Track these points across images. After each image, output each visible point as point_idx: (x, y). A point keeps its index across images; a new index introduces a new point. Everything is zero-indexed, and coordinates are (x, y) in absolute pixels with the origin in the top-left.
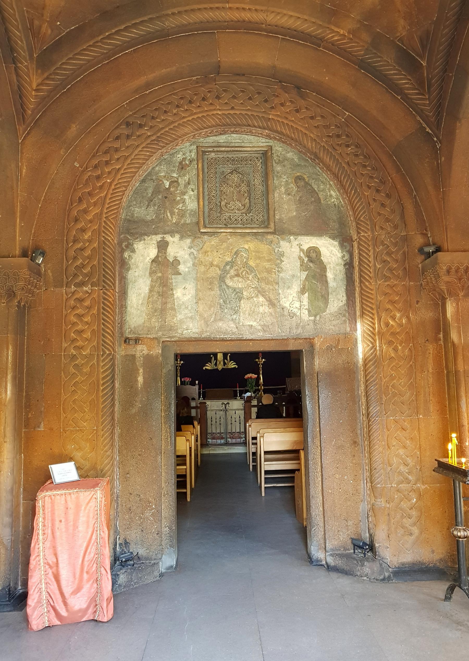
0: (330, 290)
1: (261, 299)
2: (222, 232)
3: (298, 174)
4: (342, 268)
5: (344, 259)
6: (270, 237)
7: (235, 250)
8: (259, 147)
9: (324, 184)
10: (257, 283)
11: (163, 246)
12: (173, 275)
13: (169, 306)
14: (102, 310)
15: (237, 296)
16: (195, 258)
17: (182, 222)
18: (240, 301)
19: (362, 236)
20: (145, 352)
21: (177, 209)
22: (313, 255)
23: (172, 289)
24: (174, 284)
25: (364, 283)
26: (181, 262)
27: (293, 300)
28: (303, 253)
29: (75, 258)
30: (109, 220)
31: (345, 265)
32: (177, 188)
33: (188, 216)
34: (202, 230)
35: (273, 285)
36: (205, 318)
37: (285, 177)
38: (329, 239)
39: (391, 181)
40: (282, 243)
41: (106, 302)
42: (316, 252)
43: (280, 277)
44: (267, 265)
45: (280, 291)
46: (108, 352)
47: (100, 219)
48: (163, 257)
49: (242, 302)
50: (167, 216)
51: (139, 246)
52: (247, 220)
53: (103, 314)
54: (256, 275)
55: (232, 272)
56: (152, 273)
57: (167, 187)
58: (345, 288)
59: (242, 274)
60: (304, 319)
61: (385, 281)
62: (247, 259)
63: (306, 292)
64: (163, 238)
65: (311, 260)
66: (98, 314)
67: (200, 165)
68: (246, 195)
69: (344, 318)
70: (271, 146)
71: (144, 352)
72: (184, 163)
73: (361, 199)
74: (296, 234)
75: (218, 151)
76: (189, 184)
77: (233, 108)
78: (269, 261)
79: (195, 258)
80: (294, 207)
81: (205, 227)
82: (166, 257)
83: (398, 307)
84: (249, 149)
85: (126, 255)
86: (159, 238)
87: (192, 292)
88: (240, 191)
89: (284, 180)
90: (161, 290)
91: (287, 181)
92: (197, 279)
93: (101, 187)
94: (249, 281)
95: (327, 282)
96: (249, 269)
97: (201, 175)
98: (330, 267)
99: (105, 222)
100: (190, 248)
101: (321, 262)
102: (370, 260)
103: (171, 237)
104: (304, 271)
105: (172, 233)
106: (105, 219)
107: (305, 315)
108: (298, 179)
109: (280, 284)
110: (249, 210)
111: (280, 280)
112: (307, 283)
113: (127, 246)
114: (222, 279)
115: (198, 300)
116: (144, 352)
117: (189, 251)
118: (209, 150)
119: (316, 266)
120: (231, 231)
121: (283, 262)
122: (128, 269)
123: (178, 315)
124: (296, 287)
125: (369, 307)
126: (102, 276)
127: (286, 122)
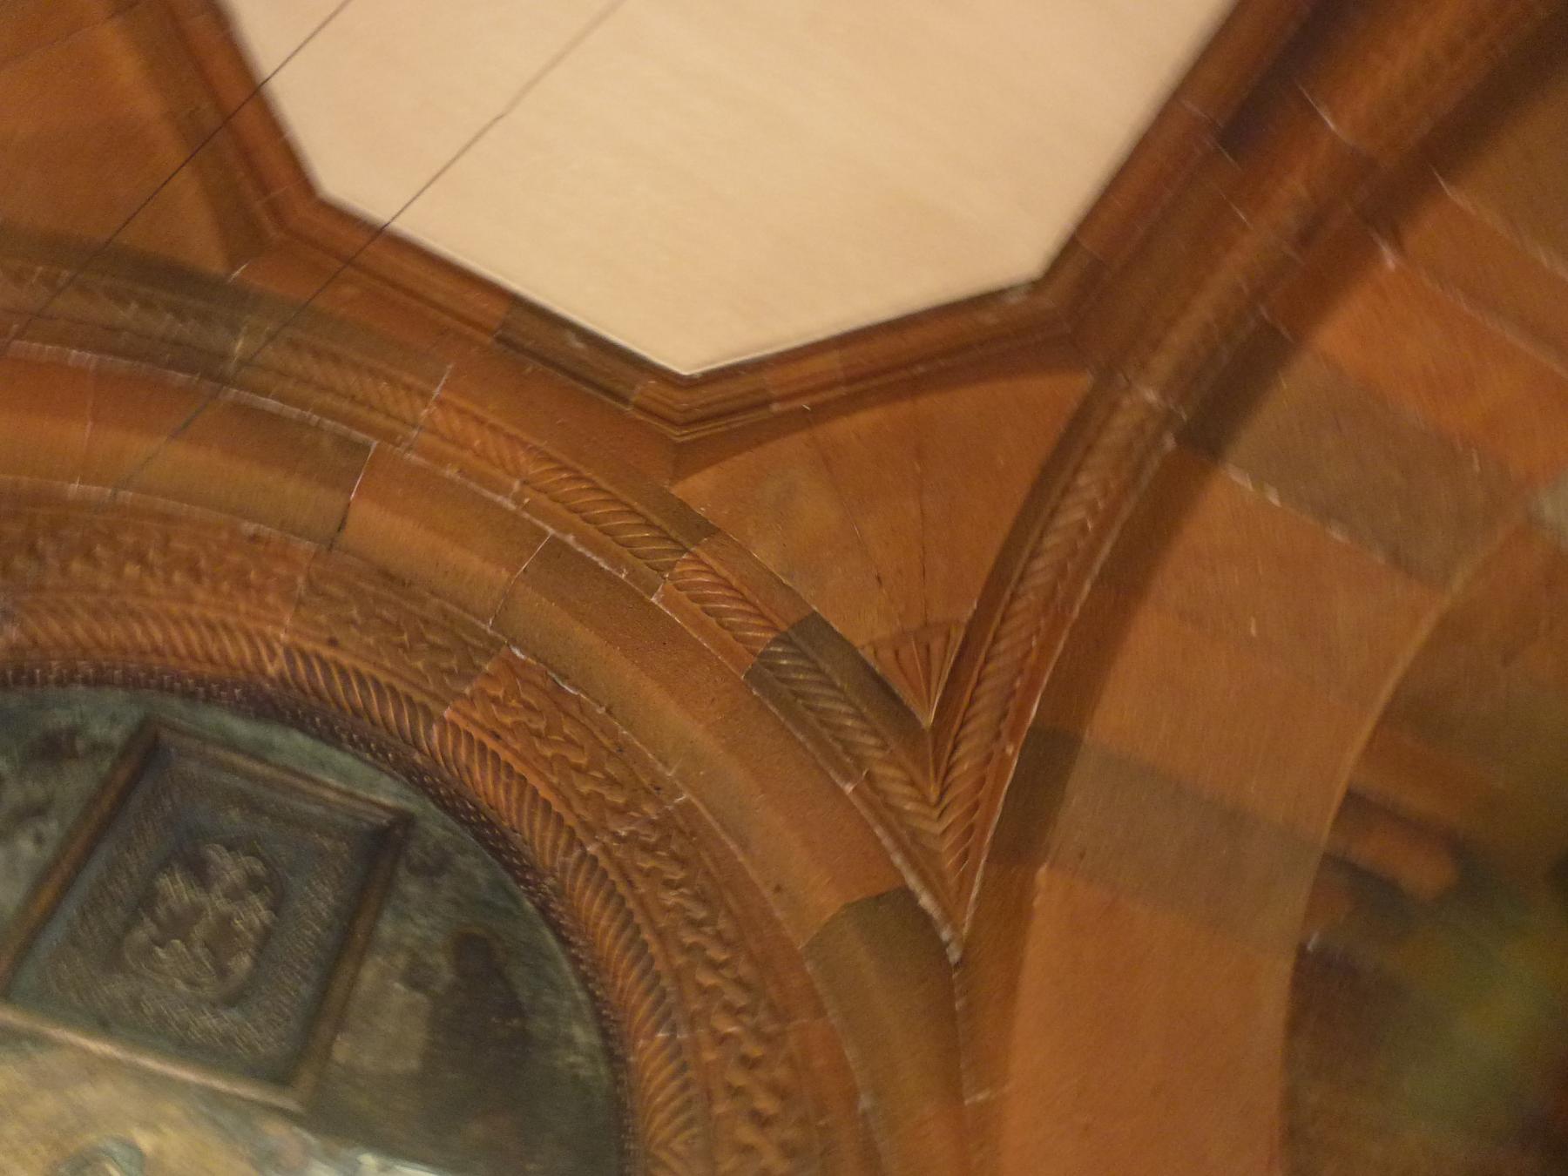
67: (123, 775)
77: (333, 643)
80: (417, 1036)
84: (331, 795)
108: (466, 946)
110: (234, 1000)
127: (491, 744)
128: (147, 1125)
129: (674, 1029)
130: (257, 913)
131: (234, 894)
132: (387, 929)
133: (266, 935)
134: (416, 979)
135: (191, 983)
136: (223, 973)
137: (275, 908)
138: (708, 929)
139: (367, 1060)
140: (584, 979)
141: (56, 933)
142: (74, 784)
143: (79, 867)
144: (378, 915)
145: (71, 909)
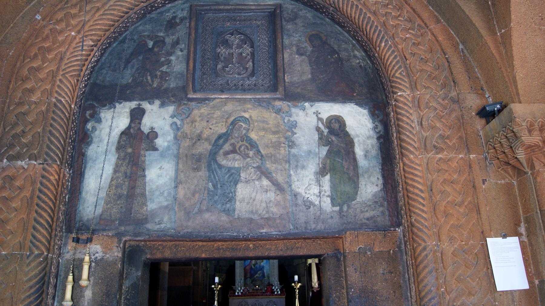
0: (360, 171)
1: (265, 182)
2: (216, 98)
3: (313, 33)
4: (374, 141)
5: (377, 130)
6: (278, 104)
7: (232, 119)
8: (265, 5)
9: (346, 43)
10: (260, 162)
11: (137, 115)
12: (147, 150)
13: (138, 191)
14: (38, 192)
15: (231, 178)
16: (178, 129)
17: (165, 86)
18: (236, 185)
19: (400, 95)
20: (99, 255)
21: (160, 71)
22: (336, 126)
23: (144, 170)
24: (147, 163)
25: (407, 156)
26: (159, 133)
27: (310, 184)
28: (323, 123)
29: (16, 124)
30: (67, 78)
31: (378, 138)
32: (162, 48)
33: (173, 79)
34: (190, 96)
35: (281, 165)
36: (185, 208)
37: (297, 35)
38: (355, 106)
39: (429, 33)
40: (293, 110)
41: (44, 181)
42: (339, 122)
43: (292, 153)
44: (274, 138)
45: (292, 172)
46: (36, 252)
47: (56, 77)
48: (136, 128)
49: (239, 186)
50: (147, 79)
51: (106, 115)
52: (249, 85)
53: (39, 197)
54: (259, 151)
55: (227, 147)
56: (120, 147)
57: (150, 47)
58: (380, 167)
59: (239, 149)
60: (326, 211)
61: (437, 153)
62: (248, 130)
63: (327, 174)
64: (139, 105)
65: (332, 132)
66: (32, 198)
67: (193, 24)
68: (249, 57)
69: (381, 209)
70: (281, 4)
71: (97, 255)
72: (173, 21)
73: (393, 52)
74: (312, 100)
75: (215, 10)
76: (177, 43)
78: (275, 133)
79: (178, 129)
80: (307, 68)
81: (195, 91)
82: (139, 129)
83: (458, 189)
84: (253, 7)
85: (89, 126)
86: (133, 104)
87: (170, 173)
88: (241, 54)
89: (296, 39)
90: (129, 171)
91: (299, 40)
92: (178, 157)
93: (63, 42)
94: (249, 159)
95: (355, 159)
96: (249, 144)
97: (193, 35)
98: (359, 141)
99: (61, 81)
100: (172, 117)
101: (347, 134)
102: (413, 126)
103: (150, 103)
104: (323, 145)
105: (150, 99)
106: (61, 77)
107: (327, 204)
108: (312, 38)
109: (291, 162)
110: (253, 74)
111: (291, 158)
112: (328, 161)
113: (92, 116)
114: (213, 155)
115: (177, 182)
116: (97, 255)
117: (170, 121)
118: (205, 8)
119: (339, 139)
120: (227, 97)
121: (296, 134)
122: (89, 144)
123: (148, 203)
124: (312, 167)
125: (418, 188)
126: (45, 147)
128: (245, 111)
129: (387, 41)
130: (247, 50)
131: (239, 47)
132: (286, 41)
133: (253, 54)
134: (300, 53)
135: (239, 74)
136: (247, 69)
137: (252, 47)
138: (389, 6)
139: (295, 79)
140: (354, 37)
141: (198, 73)
142: (181, 31)
143: (195, 54)
144: (282, 39)
145: (198, 66)
